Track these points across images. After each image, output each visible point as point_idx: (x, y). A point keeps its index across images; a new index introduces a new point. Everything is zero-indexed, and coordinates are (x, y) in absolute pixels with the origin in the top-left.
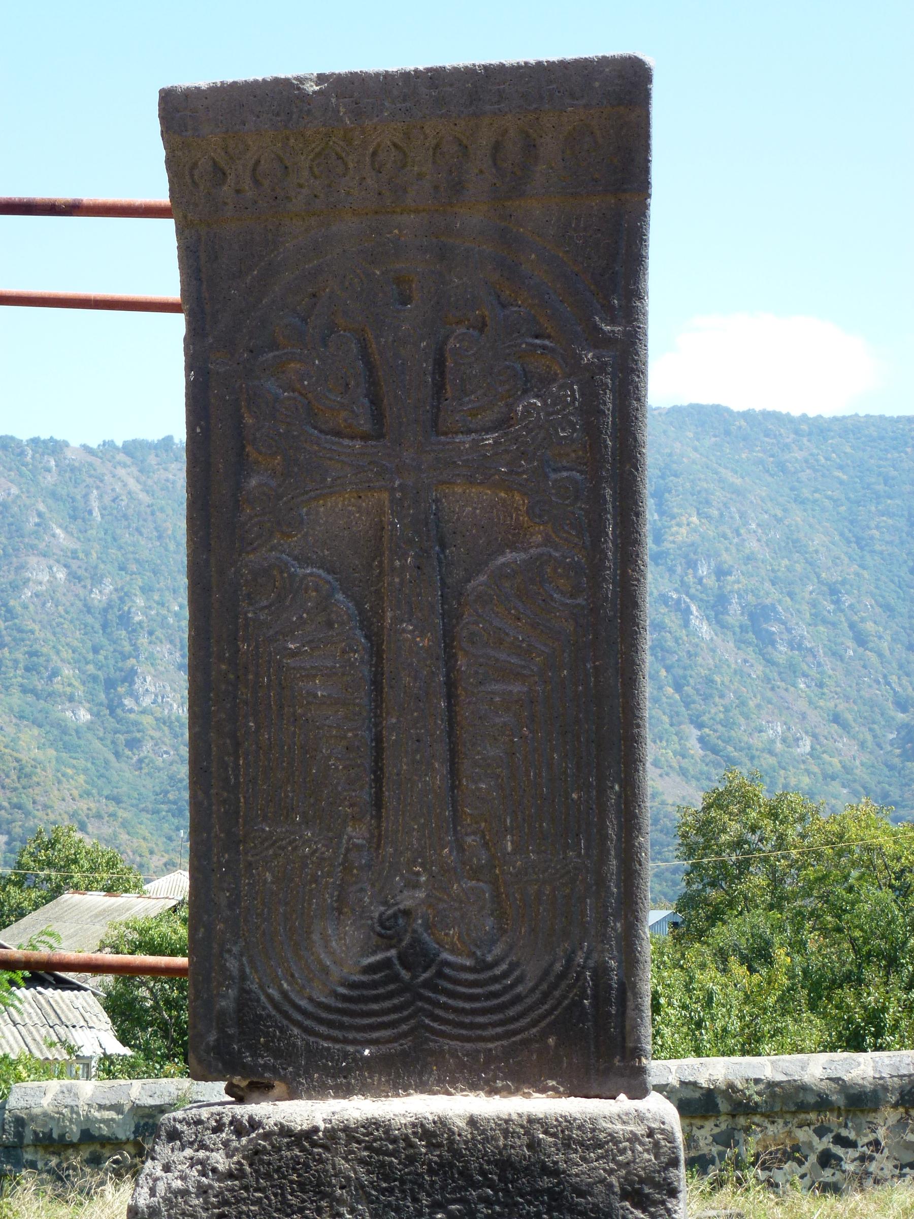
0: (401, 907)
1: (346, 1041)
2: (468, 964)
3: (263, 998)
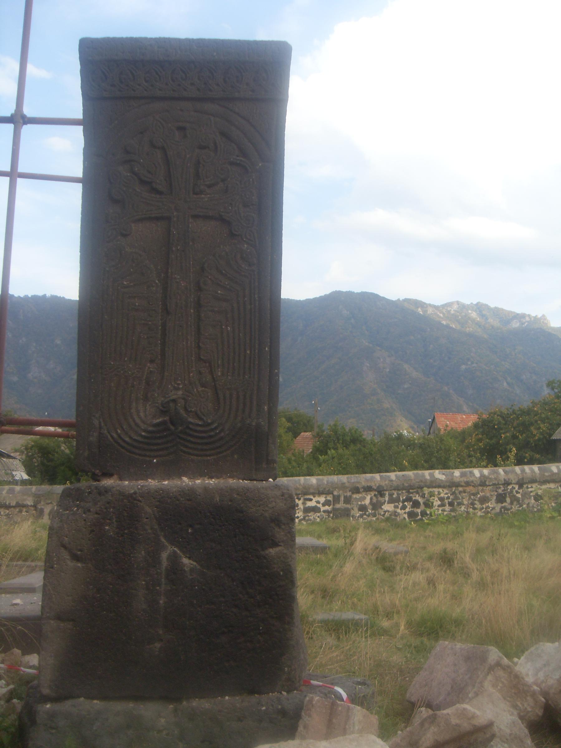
0: (171, 398)
1: (145, 456)
2: (200, 423)
3: (109, 437)
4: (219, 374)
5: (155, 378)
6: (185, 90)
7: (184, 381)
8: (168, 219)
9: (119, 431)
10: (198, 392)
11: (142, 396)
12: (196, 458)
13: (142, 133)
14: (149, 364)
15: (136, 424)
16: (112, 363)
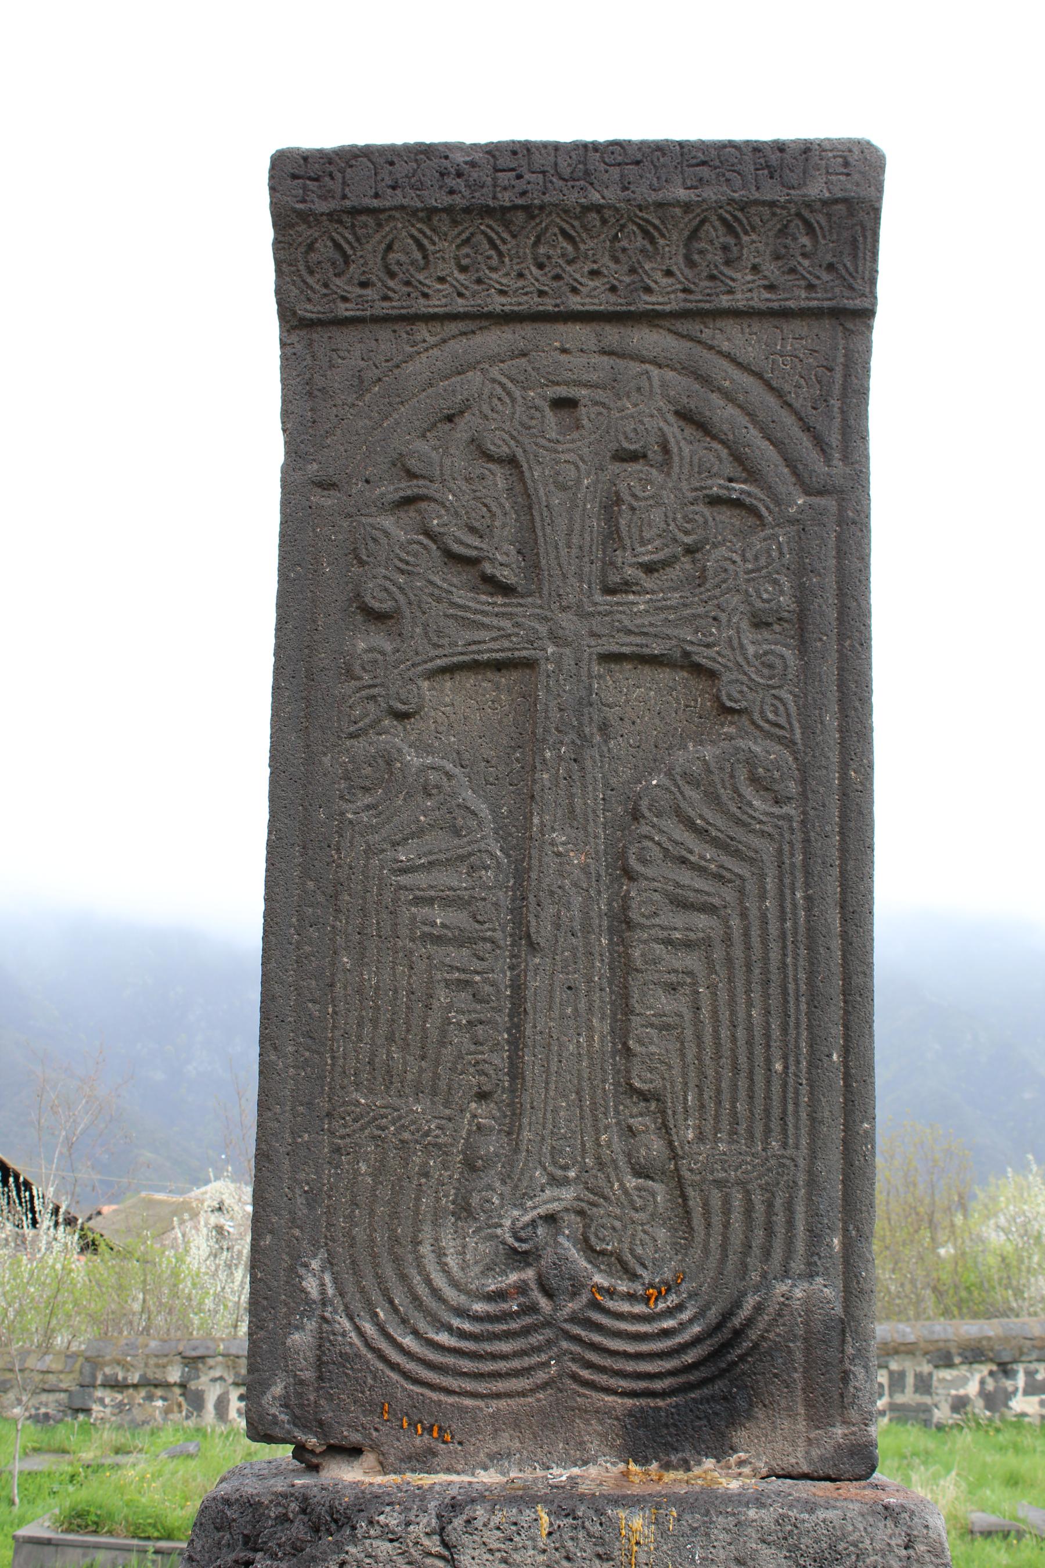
4: (690, 1135)
5: (492, 1149)
6: (574, 291)
7: (583, 1158)
8: (529, 664)
9: (381, 1314)
10: (626, 1192)
11: (453, 1202)
12: (620, 1401)
13: (450, 419)
14: (473, 1105)
15: (435, 1292)
16: (363, 1101)
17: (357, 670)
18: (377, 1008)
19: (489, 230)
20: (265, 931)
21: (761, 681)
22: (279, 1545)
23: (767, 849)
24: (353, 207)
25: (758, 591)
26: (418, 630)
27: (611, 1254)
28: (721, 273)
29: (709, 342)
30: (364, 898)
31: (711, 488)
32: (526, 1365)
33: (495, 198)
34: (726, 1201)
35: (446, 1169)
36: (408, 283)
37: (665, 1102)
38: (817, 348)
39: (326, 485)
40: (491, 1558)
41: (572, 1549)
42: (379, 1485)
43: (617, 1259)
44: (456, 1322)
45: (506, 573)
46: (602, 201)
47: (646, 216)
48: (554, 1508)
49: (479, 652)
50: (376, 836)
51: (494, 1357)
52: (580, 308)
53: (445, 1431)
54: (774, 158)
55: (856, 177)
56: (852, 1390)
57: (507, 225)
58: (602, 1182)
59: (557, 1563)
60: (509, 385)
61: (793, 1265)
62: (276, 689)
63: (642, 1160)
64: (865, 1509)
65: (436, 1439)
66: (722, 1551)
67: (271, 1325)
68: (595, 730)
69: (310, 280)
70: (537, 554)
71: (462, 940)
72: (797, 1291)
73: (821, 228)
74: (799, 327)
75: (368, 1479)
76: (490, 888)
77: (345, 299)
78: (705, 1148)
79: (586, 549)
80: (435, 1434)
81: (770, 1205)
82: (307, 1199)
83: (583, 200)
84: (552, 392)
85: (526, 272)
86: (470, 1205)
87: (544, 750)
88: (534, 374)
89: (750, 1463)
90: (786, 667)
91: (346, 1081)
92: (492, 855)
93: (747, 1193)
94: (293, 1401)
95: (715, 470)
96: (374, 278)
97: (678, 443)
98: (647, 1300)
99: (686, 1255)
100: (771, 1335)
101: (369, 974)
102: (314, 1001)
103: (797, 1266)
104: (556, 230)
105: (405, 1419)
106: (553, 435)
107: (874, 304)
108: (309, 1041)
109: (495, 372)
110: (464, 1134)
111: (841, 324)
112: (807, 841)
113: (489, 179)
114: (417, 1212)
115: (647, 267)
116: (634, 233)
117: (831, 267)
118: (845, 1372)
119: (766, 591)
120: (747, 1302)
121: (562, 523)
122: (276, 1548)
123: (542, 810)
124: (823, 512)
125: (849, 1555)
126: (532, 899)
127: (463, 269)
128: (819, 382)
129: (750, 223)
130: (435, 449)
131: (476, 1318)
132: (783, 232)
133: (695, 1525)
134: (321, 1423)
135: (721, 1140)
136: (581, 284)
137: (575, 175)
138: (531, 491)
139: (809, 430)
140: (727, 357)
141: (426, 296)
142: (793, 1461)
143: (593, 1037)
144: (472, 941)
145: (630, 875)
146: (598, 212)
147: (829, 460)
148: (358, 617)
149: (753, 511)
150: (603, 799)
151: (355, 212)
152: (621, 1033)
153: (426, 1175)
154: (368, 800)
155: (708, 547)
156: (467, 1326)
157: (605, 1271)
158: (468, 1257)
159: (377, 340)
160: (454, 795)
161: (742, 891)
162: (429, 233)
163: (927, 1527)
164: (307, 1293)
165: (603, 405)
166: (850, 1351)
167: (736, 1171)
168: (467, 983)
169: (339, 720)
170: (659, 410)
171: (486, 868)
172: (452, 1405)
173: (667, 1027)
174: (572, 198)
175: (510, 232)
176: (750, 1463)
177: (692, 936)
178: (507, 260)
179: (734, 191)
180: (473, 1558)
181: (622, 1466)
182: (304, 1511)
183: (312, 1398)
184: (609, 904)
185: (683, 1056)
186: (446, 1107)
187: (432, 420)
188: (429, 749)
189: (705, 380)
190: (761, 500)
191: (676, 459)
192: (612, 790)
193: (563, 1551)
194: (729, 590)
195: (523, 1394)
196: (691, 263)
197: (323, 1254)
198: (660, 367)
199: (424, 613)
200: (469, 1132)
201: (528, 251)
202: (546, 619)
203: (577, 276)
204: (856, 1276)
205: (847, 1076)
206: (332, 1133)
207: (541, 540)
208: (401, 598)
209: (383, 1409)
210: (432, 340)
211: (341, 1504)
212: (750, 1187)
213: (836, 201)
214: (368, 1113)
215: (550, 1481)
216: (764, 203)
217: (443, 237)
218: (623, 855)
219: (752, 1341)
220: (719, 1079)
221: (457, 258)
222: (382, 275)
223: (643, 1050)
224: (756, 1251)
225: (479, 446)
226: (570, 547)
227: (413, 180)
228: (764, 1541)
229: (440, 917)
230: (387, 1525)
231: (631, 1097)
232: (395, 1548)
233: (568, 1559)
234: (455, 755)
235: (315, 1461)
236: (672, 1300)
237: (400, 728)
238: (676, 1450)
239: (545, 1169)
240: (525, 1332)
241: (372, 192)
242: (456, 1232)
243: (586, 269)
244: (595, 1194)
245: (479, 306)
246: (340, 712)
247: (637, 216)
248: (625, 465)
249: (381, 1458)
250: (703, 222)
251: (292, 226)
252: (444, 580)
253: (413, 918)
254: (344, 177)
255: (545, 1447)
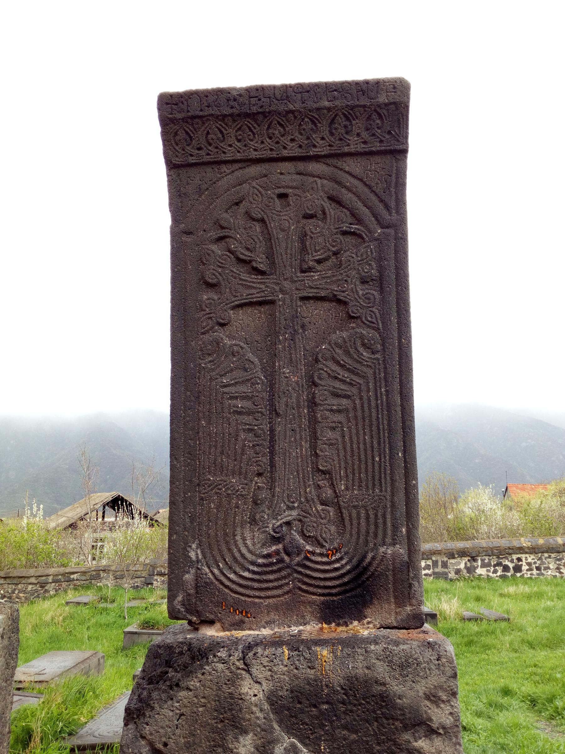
4: (343, 488)
6: (285, 148)
7: (300, 498)
8: (272, 302)
9: (221, 565)
10: (318, 512)
11: (249, 518)
12: (318, 598)
14: (256, 478)
15: (243, 555)
16: (212, 479)
17: (204, 307)
18: (216, 441)
19: (248, 124)
20: (171, 412)
21: (365, 305)
22: (178, 666)
23: (370, 372)
24: (192, 116)
25: (363, 269)
26: (227, 290)
27: (313, 537)
28: (344, 137)
29: (341, 167)
30: (210, 398)
31: (343, 228)
32: (280, 584)
33: (250, 109)
34: (358, 514)
35: (246, 504)
36: (217, 148)
37: (332, 475)
38: (385, 167)
39: (188, 233)
40: (264, 669)
41: (298, 665)
42: (221, 637)
43: (315, 539)
44: (251, 567)
45: (262, 266)
46: (294, 108)
47: (312, 114)
48: (290, 647)
49: (252, 298)
50: (214, 373)
51: (267, 581)
52: (287, 155)
53: (248, 613)
54: (364, 87)
55: (399, 93)
56: (413, 591)
57: (256, 121)
58: (308, 508)
59: (292, 670)
60: (260, 189)
61: (387, 540)
62: (172, 316)
63: (324, 498)
64: (420, 644)
65: (244, 616)
66: (360, 664)
67: (177, 572)
68: (299, 328)
69: (177, 148)
70: (274, 258)
71: (249, 413)
72: (389, 550)
73: (385, 116)
74: (377, 159)
75: (216, 634)
76: (260, 392)
77: (191, 155)
78: (349, 493)
79: (293, 255)
80: (244, 614)
81: (376, 515)
82: (190, 519)
83: (286, 108)
84: (278, 191)
85: (265, 141)
86: (255, 519)
87: (279, 336)
88: (270, 184)
89: (373, 623)
90: (375, 299)
91: (205, 471)
92: (260, 379)
93: (367, 510)
94: (186, 603)
95: (344, 220)
96: (203, 146)
97: (329, 210)
98: (327, 556)
99: (343, 537)
100: (379, 569)
101: (213, 428)
102: (191, 439)
103: (388, 540)
104: (276, 122)
105: (232, 608)
106: (279, 209)
107: (407, 147)
108: (190, 456)
109: (254, 184)
110: (252, 490)
111: (394, 157)
112: (385, 368)
113: (247, 101)
114: (234, 523)
115: (314, 137)
116: (308, 122)
117: (389, 133)
118: (410, 584)
119: (366, 268)
120: (369, 556)
121: (283, 245)
122: (177, 667)
123: (279, 360)
124: (389, 235)
125: (413, 664)
126: (276, 395)
127: (239, 141)
128: (386, 181)
129: (355, 115)
130: (231, 217)
131: (259, 565)
132: (369, 118)
133: (349, 653)
134: (197, 612)
135: (355, 489)
136: (287, 145)
137: (283, 98)
138: (270, 232)
139: (382, 202)
140: (348, 173)
141: (224, 153)
142: (390, 621)
143: (302, 449)
144: (253, 413)
145: (315, 384)
146: (293, 113)
147: (391, 213)
148: (204, 286)
149: (360, 236)
150: (304, 355)
151: (193, 117)
152: (314, 447)
153: (238, 507)
154: (210, 359)
155: (342, 252)
156: (256, 569)
157: (311, 544)
158: (255, 540)
159: (205, 172)
160: (244, 355)
161: (360, 390)
162: (224, 126)
163: (446, 651)
164: (191, 558)
165: (299, 196)
166: (412, 575)
167: (362, 502)
168: (252, 430)
169: (197, 327)
170: (321, 196)
171: (258, 384)
172: (250, 602)
173: (331, 444)
174: (282, 108)
175: (257, 124)
176: (373, 623)
177: (341, 408)
178: (256, 136)
179: (348, 102)
180: (257, 670)
181: (320, 625)
182: (189, 650)
183: (194, 601)
184: (307, 396)
185: (338, 456)
186: (245, 480)
187: (230, 204)
188: (234, 338)
189: (339, 183)
190: (363, 231)
191: (328, 216)
192: (307, 351)
193: (294, 665)
194: (351, 269)
195: (279, 596)
196: (332, 134)
197: (197, 542)
198: (321, 178)
199: (230, 283)
200: (255, 489)
201: (265, 132)
202: (278, 284)
203: (286, 142)
204: (413, 544)
205: (405, 462)
206: (200, 492)
207: (275, 252)
208: (220, 278)
209: (222, 604)
210: (228, 171)
211: (203, 648)
212: (368, 508)
213: (391, 104)
214: (214, 483)
215: (291, 633)
216: (361, 106)
217: (230, 127)
218: (312, 377)
219: (371, 572)
220: (353, 464)
221: (236, 136)
222: (206, 145)
223: (323, 454)
224: (371, 534)
225: (249, 215)
226: (287, 255)
227: (216, 103)
228: (378, 659)
229: (241, 404)
230: (221, 657)
231: (319, 473)
232: (225, 666)
233: (296, 669)
234: (244, 339)
235: (196, 626)
236: (338, 555)
237: (222, 330)
238: (342, 618)
239: (285, 503)
240: (279, 570)
241: (199, 109)
242: (250, 530)
243: (289, 138)
244: (306, 513)
245: (246, 156)
246: (198, 324)
247: (309, 114)
248: (308, 220)
249: (222, 625)
250: (336, 116)
251: (167, 125)
252: (237, 270)
253: (230, 405)
254: (187, 103)
255: (289, 618)
